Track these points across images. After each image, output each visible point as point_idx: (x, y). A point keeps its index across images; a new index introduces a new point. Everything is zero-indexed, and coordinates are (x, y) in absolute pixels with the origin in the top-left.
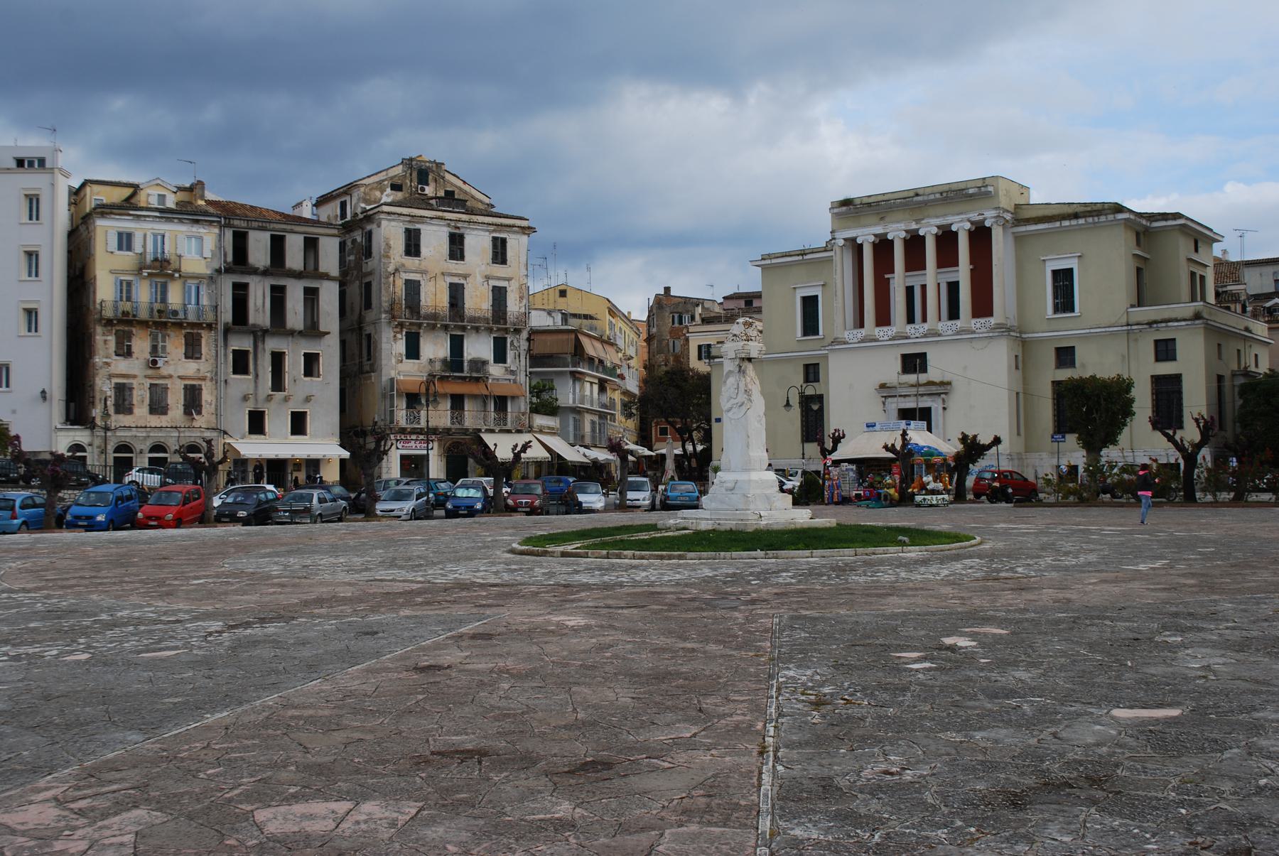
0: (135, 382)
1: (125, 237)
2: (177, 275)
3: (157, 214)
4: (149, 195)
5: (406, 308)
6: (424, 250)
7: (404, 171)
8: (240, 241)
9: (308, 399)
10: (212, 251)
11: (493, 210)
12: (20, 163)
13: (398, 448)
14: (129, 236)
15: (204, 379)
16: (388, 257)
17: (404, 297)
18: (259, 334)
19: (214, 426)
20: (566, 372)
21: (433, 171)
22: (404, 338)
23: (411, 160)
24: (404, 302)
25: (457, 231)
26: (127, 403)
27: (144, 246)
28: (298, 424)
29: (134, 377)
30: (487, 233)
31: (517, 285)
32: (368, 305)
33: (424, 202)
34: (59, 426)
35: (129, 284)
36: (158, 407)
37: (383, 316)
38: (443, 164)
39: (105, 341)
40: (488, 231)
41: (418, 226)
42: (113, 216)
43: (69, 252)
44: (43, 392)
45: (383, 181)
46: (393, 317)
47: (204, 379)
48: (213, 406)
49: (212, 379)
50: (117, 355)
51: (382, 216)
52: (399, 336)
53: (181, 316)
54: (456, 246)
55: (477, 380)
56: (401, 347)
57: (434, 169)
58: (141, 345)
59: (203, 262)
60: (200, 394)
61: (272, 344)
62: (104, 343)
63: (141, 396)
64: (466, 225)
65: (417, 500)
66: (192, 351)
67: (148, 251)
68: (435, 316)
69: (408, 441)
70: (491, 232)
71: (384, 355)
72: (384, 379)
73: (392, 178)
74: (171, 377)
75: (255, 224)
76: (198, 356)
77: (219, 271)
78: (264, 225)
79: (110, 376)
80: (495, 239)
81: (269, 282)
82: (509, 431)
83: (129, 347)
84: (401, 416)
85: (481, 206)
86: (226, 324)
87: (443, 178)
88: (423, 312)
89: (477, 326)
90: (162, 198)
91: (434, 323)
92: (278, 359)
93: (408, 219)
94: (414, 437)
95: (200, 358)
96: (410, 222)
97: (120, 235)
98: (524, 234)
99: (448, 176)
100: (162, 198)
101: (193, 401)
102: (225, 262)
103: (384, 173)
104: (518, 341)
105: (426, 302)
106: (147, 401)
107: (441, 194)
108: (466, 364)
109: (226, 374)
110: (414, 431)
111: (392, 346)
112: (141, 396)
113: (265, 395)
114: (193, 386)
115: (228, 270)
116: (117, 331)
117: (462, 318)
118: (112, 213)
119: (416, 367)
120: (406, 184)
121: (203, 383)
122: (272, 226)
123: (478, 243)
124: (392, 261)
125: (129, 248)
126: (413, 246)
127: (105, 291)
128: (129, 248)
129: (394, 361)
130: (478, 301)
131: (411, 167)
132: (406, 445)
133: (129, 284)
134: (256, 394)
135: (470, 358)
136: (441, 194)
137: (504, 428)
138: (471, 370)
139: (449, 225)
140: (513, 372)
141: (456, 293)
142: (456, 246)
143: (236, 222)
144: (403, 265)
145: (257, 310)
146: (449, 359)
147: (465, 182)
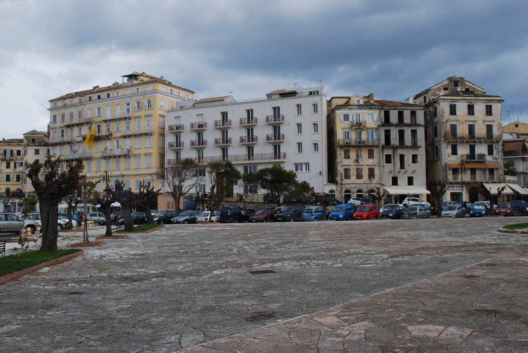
0: (351, 168)
1: (346, 116)
2: (365, 128)
3: (357, 107)
4: (354, 100)
5: (451, 135)
6: (458, 112)
7: (448, 82)
8: (387, 114)
9: (414, 172)
10: (377, 119)
11: (486, 94)
12: (311, 93)
13: (449, 190)
14: (348, 115)
15: (375, 165)
16: (443, 116)
17: (450, 131)
18: (395, 148)
19: (379, 182)
20: (519, 158)
21: (460, 81)
22: (451, 147)
23: (451, 78)
24: (450, 133)
25: (471, 104)
26: (348, 175)
27: (353, 119)
28: (410, 181)
29: (351, 166)
30: (483, 104)
31: (497, 124)
32: (436, 135)
33: (457, 94)
34: (326, 184)
35: (348, 133)
36: (359, 176)
37: (442, 139)
38: (464, 78)
39: (340, 153)
40: (484, 103)
41: (455, 103)
42: (342, 109)
43: (328, 123)
44: (320, 172)
45: (440, 87)
46: (446, 139)
47: (375, 165)
48: (379, 175)
49: (378, 166)
50: (345, 158)
51: (440, 100)
52: (449, 146)
53: (366, 143)
54: (471, 110)
55: (481, 162)
56: (449, 150)
57: (461, 80)
58: (353, 154)
59: (374, 123)
60: (374, 171)
61: (400, 152)
62: (340, 154)
63: (353, 173)
64: (474, 101)
65: (458, 210)
66: (371, 155)
67: (354, 120)
68: (463, 138)
69: (453, 187)
70: (485, 103)
71: (443, 154)
72: (443, 163)
73: (443, 86)
74: (363, 165)
75: (392, 108)
76: (373, 157)
77: (379, 126)
78: (395, 108)
79: (343, 166)
80: (487, 106)
81: (398, 128)
82: (495, 182)
83: (349, 155)
84: (450, 177)
85: (480, 93)
86: (383, 145)
87: (464, 83)
88: (458, 136)
89: (480, 141)
90: (358, 101)
91: (463, 140)
92: (402, 157)
93: (451, 101)
94: (456, 185)
95: (373, 158)
96: (451, 102)
97: (344, 115)
98: (499, 103)
99: (466, 83)
100: (358, 101)
102: (382, 122)
103: (440, 84)
104: (498, 146)
105: (459, 132)
106: (355, 174)
107: (464, 90)
108: (476, 156)
109: (383, 163)
110: (456, 183)
111: (446, 150)
112: (353, 173)
113: (398, 171)
114: (371, 168)
115: (383, 125)
116: (344, 149)
117: (474, 138)
118: (341, 108)
119: (456, 158)
120: (449, 87)
121: (375, 167)
122: (399, 108)
123: (480, 108)
124: (445, 117)
125: (348, 120)
126: (453, 111)
127: (340, 136)
128: (348, 120)
129: (447, 156)
130: (480, 131)
131: (451, 81)
132: (453, 188)
133: (348, 133)
134: (394, 171)
135: (478, 153)
136: (464, 90)
137: (493, 181)
138: (479, 158)
139: (467, 102)
140: (496, 159)
141: (471, 128)
142: (471, 110)
143: (385, 108)
144: (449, 119)
145: (394, 139)
146: (469, 154)
147: (473, 84)
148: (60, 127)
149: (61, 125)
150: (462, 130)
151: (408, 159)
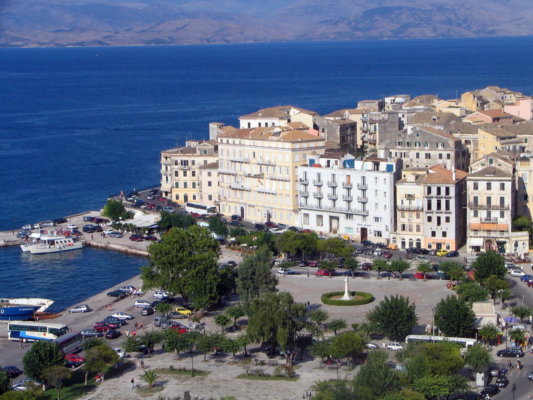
54: (489, 187)
62: (399, 214)
66: (418, 217)
68: (482, 206)
75: (433, 185)
79: (401, 222)
101: (418, 230)
111: (470, 213)
123: (496, 185)
126: (476, 187)
127: (399, 203)
130: (495, 202)
141: (489, 199)
142: (489, 187)
148: (227, 160)
149: (227, 158)
150: (482, 201)
151: (443, 220)
